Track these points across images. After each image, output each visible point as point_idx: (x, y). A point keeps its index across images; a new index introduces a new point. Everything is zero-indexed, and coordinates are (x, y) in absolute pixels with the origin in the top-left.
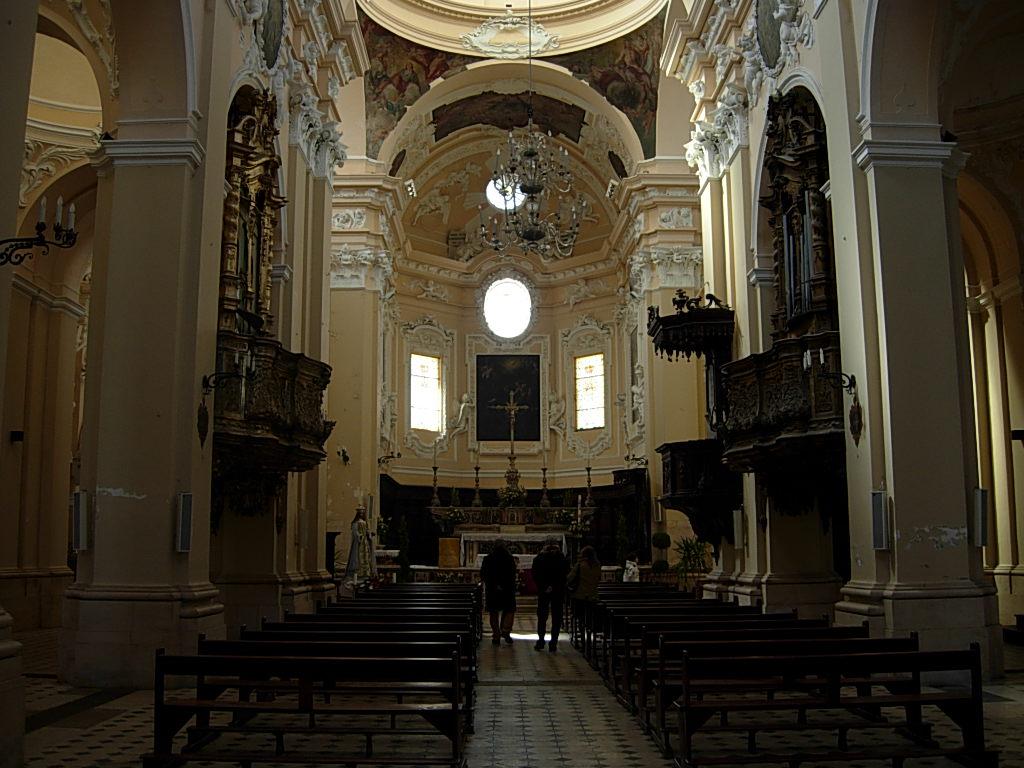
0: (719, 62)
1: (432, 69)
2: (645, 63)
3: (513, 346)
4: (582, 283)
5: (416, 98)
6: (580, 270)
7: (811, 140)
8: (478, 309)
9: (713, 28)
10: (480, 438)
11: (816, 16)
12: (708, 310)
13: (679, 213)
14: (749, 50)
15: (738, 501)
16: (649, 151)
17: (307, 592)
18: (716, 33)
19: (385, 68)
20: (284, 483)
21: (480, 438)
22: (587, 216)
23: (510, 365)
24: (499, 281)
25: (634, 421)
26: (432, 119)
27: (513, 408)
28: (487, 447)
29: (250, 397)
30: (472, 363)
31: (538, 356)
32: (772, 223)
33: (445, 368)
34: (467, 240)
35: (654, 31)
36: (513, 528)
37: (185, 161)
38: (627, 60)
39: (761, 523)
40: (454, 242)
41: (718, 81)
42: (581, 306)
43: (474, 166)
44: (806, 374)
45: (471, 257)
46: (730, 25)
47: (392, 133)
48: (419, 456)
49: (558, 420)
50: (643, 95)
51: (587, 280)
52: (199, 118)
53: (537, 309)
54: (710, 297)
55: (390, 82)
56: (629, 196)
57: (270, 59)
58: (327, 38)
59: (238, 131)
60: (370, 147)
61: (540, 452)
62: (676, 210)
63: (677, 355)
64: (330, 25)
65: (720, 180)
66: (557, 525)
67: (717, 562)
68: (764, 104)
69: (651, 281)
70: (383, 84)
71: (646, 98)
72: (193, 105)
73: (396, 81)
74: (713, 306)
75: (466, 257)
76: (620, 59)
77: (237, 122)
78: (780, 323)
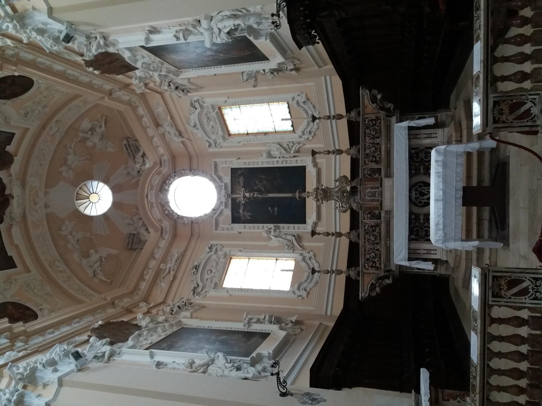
4: (161, 130)
6: (151, 131)
8: (193, 223)
10: (302, 220)
21: (302, 220)
22: (101, 127)
28: (311, 217)
30: (238, 227)
31: (232, 169)
33: (239, 253)
34: (135, 232)
36: (387, 194)
42: (182, 129)
43: (64, 228)
45: (147, 229)
48: (317, 283)
49: (285, 149)
51: (158, 125)
53: (192, 170)
61: (315, 165)
75: (145, 233)
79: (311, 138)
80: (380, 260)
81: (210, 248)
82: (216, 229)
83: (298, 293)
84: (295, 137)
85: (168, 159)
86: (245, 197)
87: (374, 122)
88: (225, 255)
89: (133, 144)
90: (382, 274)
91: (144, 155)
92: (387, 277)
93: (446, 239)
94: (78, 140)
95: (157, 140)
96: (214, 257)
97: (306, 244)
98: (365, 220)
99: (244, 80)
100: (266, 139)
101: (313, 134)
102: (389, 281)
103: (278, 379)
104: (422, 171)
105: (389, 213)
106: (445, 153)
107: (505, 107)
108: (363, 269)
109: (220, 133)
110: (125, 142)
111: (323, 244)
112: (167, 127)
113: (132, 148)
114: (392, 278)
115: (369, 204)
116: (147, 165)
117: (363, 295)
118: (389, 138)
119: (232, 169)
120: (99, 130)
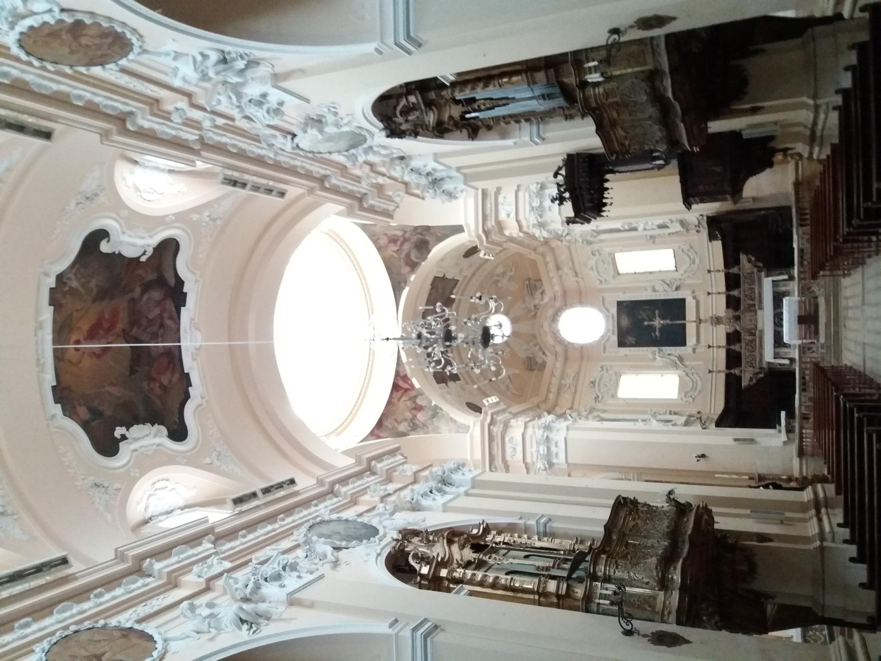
0: (374, 181)
1: (406, 386)
2: (395, 235)
3: (611, 321)
4: (561, 272)
5: (427, 397)
6: (552, 274)
7: (412, 99)
8: (582, 348)
9: (350, 187)
10: (682, 343)
11: (307, 101)
12: (566, 178)
13: (503, 204)
14: (356, 158)
15: (735, 135)
16: (458, 229)
17: (828, 514)
18: (353, 185)
19: (405, 420)
20: (725, 534)
21: (682, 343)
23: (625, 322)
24: (561, 332)
25: (667, 227)
26: (444, 384)
27: (658, 323)
29: (643, 583)
32: (489, 128)
33: (628, 372)
34: (532, 356)
37: (429, 640)
38: (395, 248)
39: (755, 111)
40: (533, 365)
41: (389, 181)
42: (578, 270)
44: (608, 79)
45: (544, 353)
46: (346, 175)
47: (452, 415)
48: (700, 392)
49: (668, 285)
50: (419, 236)
51: (558, 268)
52: (396, 621)
54: (556, 175)
55: (415, 416)
56: (493, 243)
57: (371, 532)
58: (368, 476)
59: (420, 569)
60: (461, 431)
61: (694, 298)
62: (500, 207)
63: (607, 198)
64: (358, 475)
65: (465, 175)
66: (756, 282)
67: (792, 149)
68: (396, 142)
70: (417, 422)
71: (421, 234)
72: (381, 627)
73: (415, 412)
74: (563, 172)
75: (543, 356)
76: (394, 254)
77: (413, 571)
78: (572, 112)
79: (691, 276)
81: (602, 367)
82: (604, 352)
83: (685, 399)
84: (677, 275)
86: (660, 323)
88: (616, 373)
90: (757, 370)
91: (543, 293)
92: (761, 373)
93: (790, 339)
95: (555, 280)
96: (606, 375)
97: (687, 363)
100: (651, 277)
102: (762, 376)
103: (701, 421)
105: (762, 332)
106: (789, 301)
107: (806, 289)
109: (612, 273)
110: (527, 282)
111: (701, 363)
112: (566, 270)
115: (749, 327)
116: (545, 301)
118: (760, 286)
120: (509, 274)
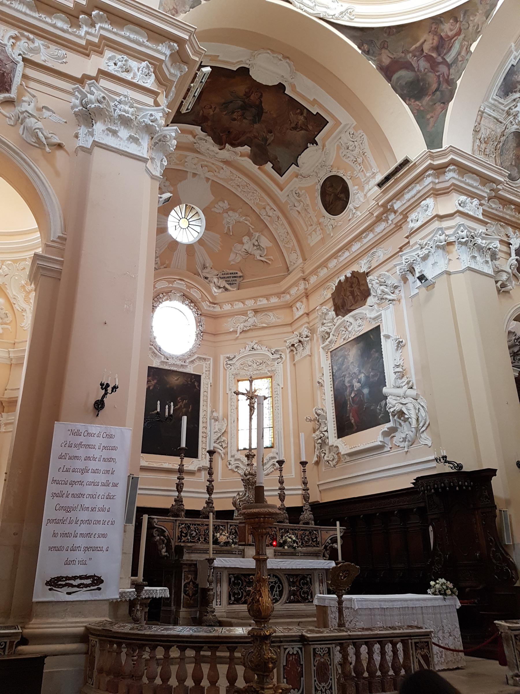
3: (179, 363)
4: (251, 314)
6: (250, 303)
22: (261, 256)
23: (174, 381)
31: (200, 376)
35: (477, 10)
38: (426, 48)
42: (250, 334)
53: (202, 334)
69: (448, 263)
76: (418, 44)
79: (230, 467)
80: (188, 542)
85: (215, 311)
87: (315, 540)
89: (236, 280)
94: (251, 229)
95: (239, 306)
98: (229, 527)
99: (317, 410)
101: (236, 470)
104: (292, 589)
108: (179, 522)
110: (240, 274)
112: (252, 320)
113: (232, 279)
114: (166, 556)
116: (214, 289)
117: (156, 520)
119: (200, 376)
120: (257, 253)
